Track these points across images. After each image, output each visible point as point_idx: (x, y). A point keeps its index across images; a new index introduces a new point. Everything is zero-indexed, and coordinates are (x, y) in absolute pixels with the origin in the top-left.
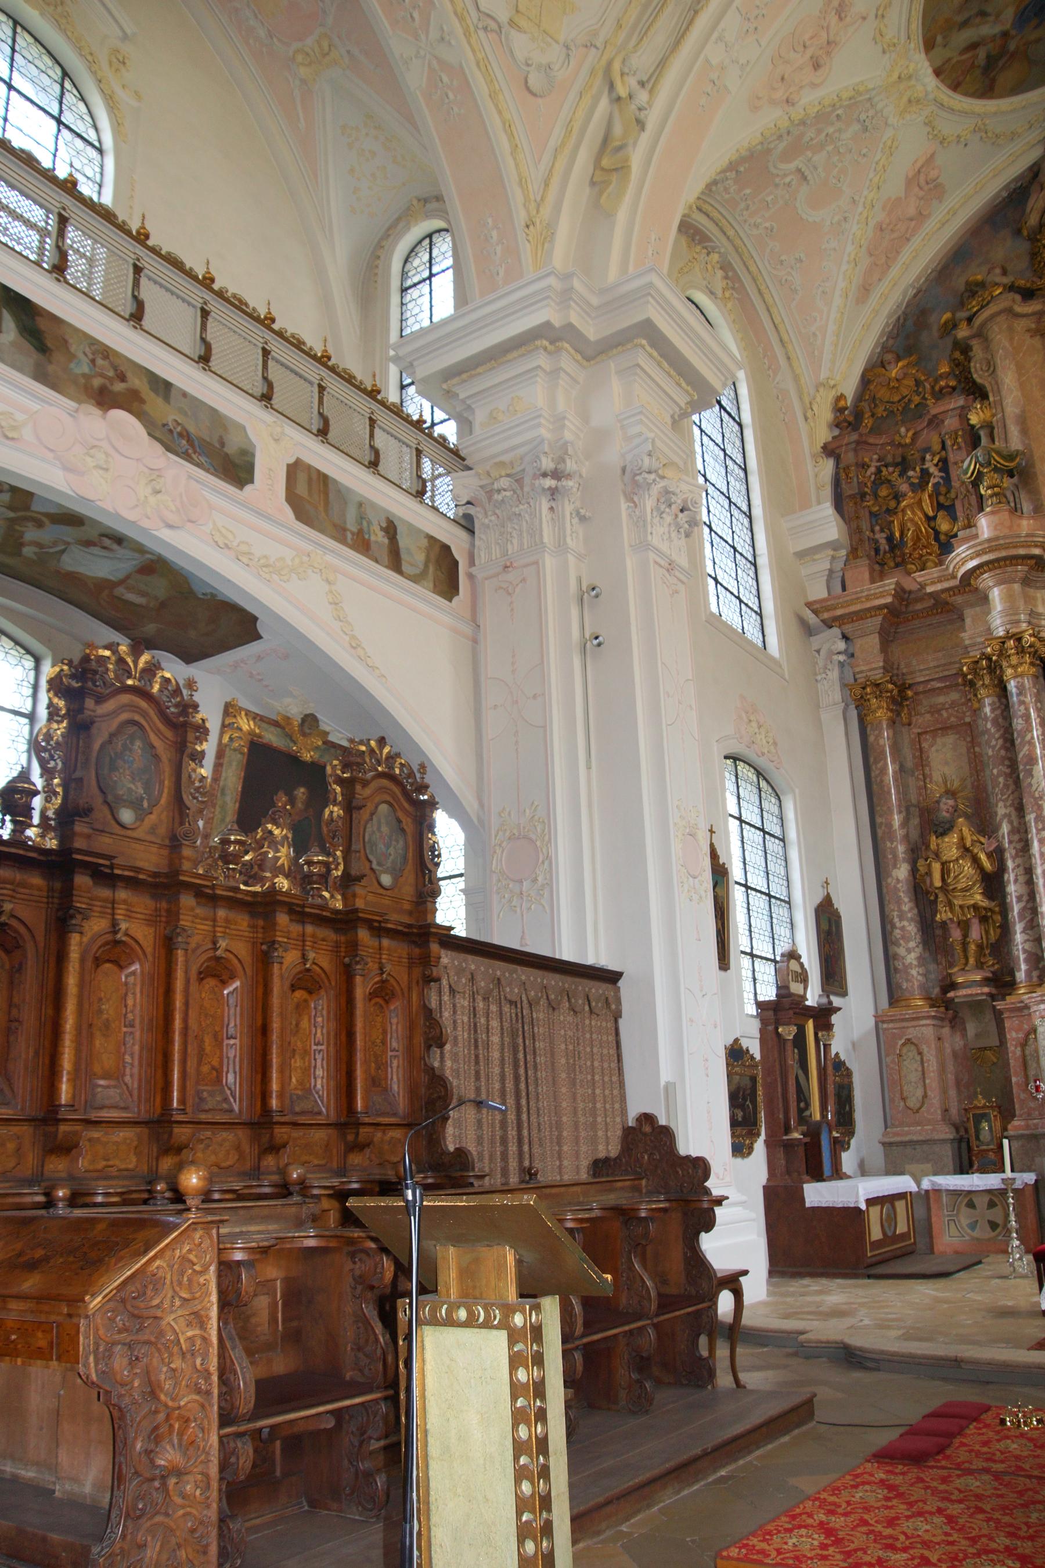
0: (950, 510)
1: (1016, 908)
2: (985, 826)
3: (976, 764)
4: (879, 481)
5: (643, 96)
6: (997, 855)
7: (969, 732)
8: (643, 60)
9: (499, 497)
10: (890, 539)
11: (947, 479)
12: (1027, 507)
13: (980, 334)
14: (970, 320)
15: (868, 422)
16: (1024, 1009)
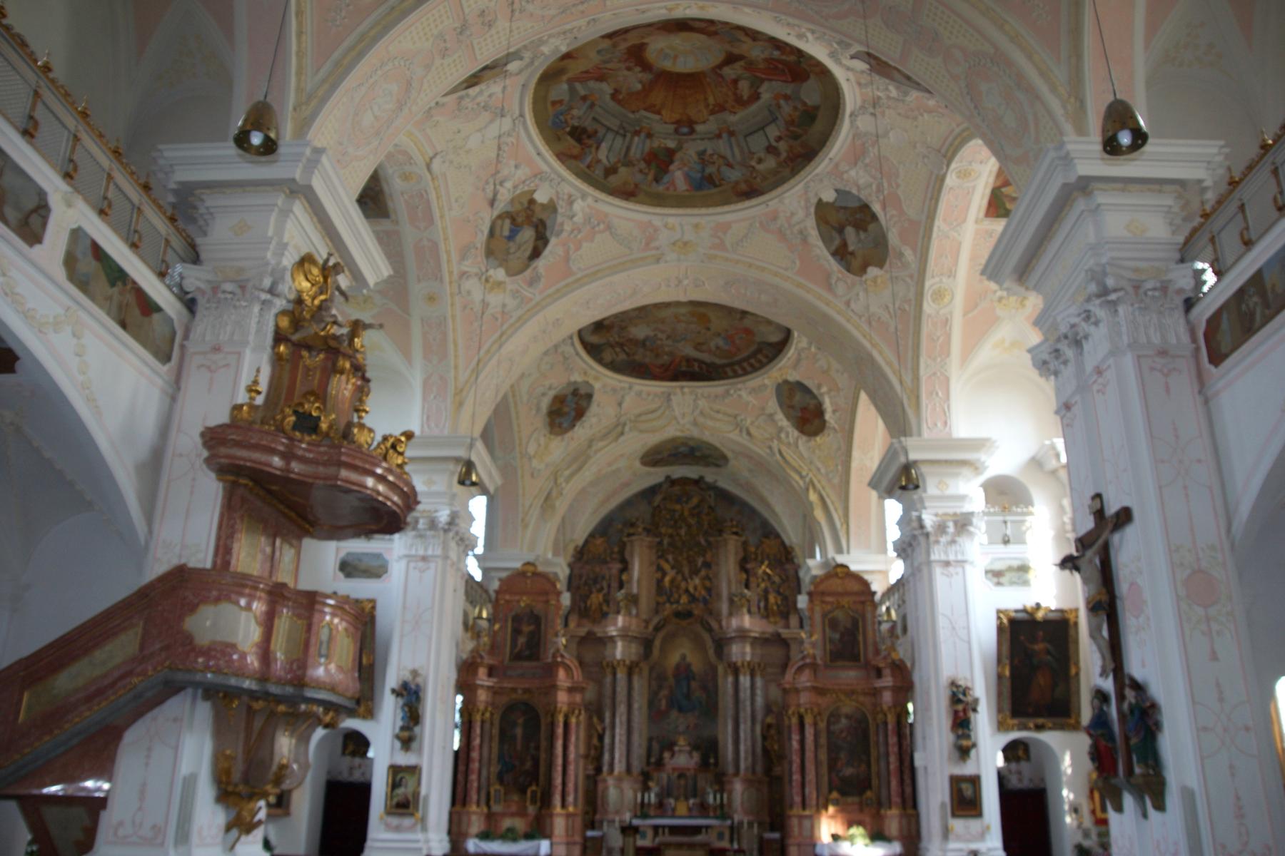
0: (607, 601)
1: (607, 747)
2: (601, 719)
3: (600, 695)
4: (586, 583)
5: (564, 485)
6: (604, 730)
7: (600, 683)
8: (567, 473)
9: (222, 296)
10: (585, 607)
11: (609, 592)
12: (634, 612)
13: (632, 542)
14: (629, 535)
15: (585, 557)
16: (605, 781)
